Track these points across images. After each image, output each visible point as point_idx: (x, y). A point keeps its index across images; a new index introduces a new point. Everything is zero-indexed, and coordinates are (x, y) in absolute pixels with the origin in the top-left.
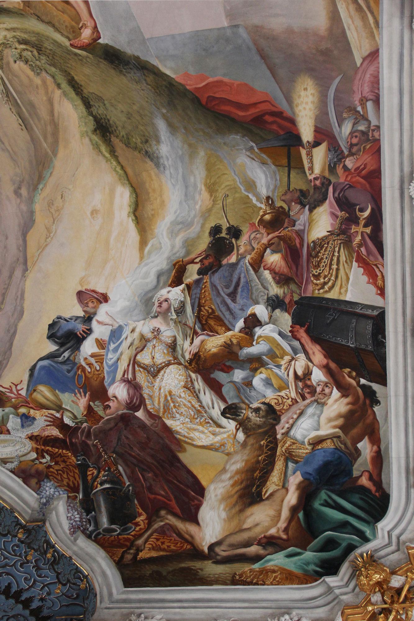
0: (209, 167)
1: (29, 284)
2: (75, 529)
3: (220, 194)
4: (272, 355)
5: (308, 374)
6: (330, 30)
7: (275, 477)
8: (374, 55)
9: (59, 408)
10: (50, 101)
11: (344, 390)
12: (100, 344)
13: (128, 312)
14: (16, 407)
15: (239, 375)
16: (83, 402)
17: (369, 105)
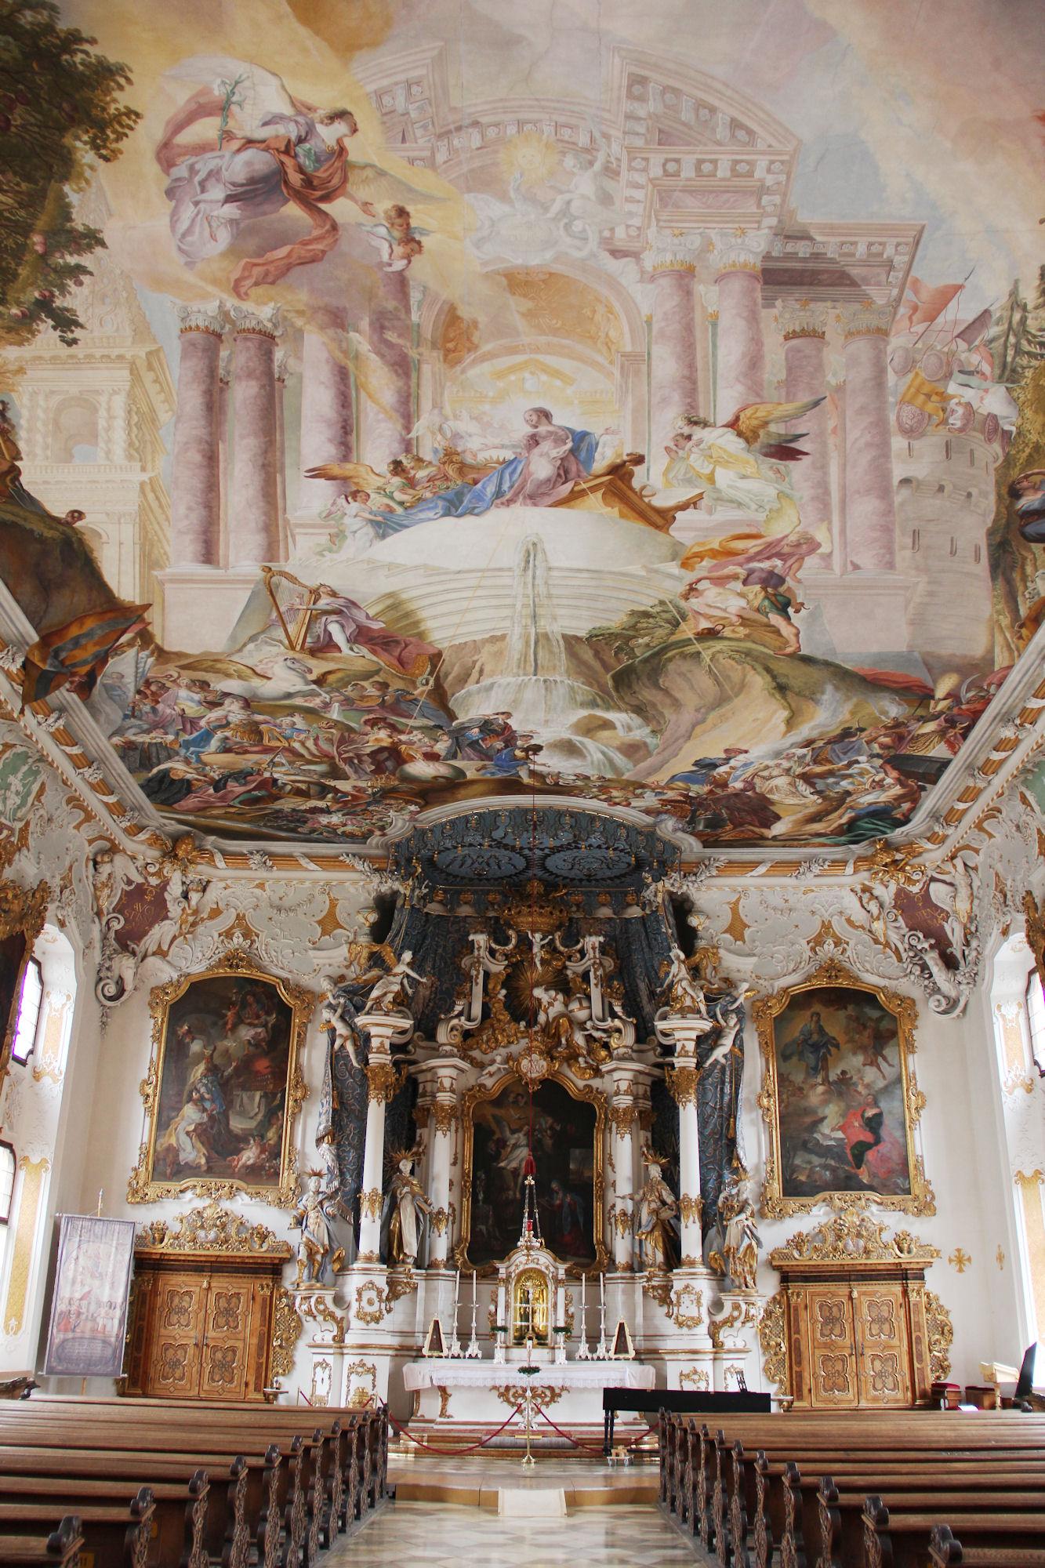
0: (856, 706)
1: (688, 744)
2: (675, 830)
3: (859, 715)
4: (861, 774)
5: (883, 780)
6: (983, 658)
7: (836, 814)
8: (1010, 667)
9: (689, 790)
10: (745, 676)
11: (903, 785)
12: (732, 768)
13: (763, 757)
14: (653, 790)
15: (831, 780)
16: (707, 788)
17: (993, 687)
